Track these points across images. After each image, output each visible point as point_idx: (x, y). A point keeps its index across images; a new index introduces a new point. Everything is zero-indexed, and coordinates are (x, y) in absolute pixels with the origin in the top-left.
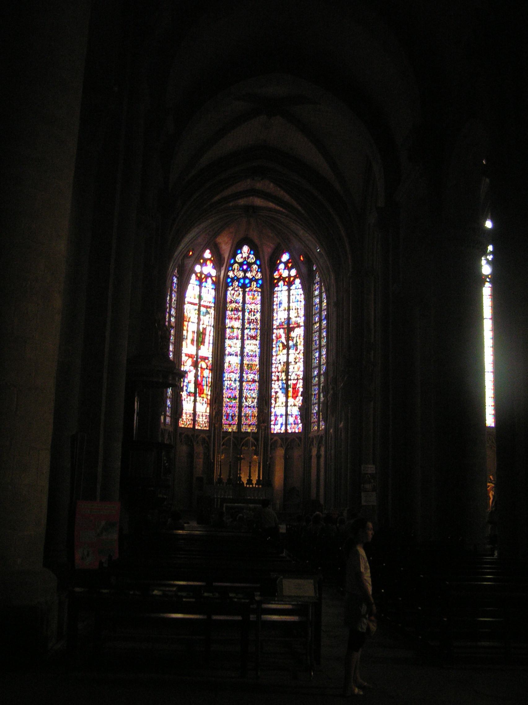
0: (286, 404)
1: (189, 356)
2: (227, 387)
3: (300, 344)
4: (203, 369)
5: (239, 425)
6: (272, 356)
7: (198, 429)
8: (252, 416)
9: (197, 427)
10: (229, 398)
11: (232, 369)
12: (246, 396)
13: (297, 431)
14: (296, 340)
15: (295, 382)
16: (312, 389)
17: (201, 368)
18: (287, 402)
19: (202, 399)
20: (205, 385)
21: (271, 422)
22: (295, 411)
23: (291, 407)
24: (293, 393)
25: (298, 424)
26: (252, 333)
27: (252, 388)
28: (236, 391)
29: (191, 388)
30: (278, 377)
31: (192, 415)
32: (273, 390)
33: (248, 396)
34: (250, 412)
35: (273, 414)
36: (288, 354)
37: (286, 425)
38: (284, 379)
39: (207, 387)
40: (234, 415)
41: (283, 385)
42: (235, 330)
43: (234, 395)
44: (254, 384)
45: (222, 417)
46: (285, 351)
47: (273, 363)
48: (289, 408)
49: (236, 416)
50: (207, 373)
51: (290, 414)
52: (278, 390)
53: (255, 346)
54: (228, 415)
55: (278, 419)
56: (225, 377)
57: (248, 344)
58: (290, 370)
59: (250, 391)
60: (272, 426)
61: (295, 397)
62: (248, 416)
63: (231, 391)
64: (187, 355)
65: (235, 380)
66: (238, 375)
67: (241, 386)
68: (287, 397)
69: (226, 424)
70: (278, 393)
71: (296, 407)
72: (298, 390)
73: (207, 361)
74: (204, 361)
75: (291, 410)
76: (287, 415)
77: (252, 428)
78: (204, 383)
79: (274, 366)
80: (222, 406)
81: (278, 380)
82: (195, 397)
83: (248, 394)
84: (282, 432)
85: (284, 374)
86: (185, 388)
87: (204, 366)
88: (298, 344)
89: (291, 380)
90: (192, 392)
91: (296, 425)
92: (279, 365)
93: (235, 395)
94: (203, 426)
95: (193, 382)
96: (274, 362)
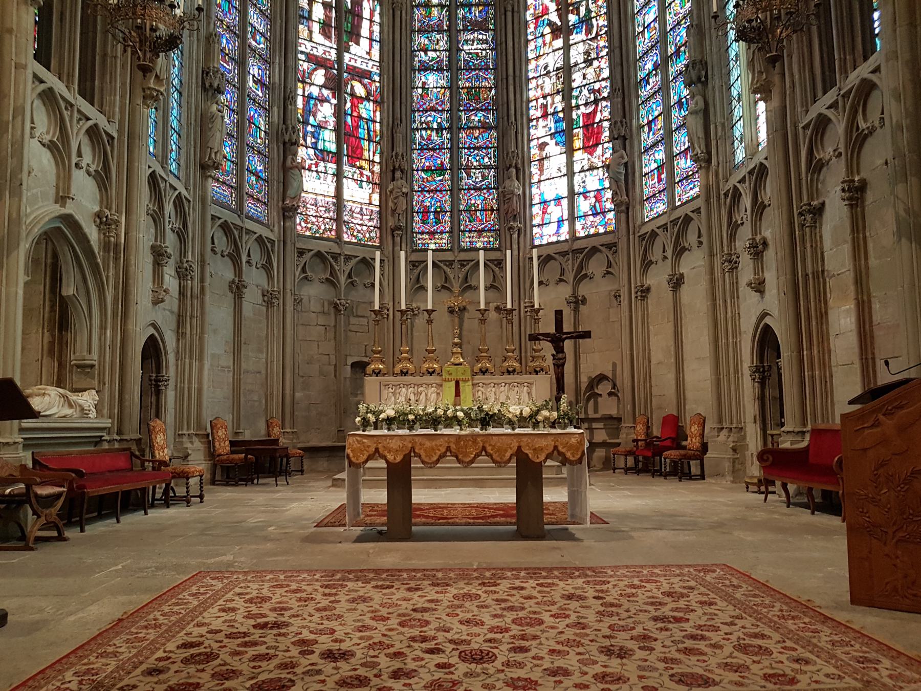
0: (567, 170)
1: (319, 62)
2: (419, 144)
3: (598, 15)
4: (358, 98)
5: (455, 232)
6: (528, 61)
7: (350, 243)
8: (485, 210)
9: (346, 238)
10: (426, 170)
11: (432, 100)
12: (467, 165)
13: (602, 230)
14: (587, 6)
15: (590, 109)
16: (643, 112)
17: (353, 95)
18: (570, 164)
19: (358, 172)
20: (364, 139)
21: (531, 220)
22: (594, 181)
23: (582, 174)
24: (587, 138)
25: (604, 213)
26: (476, 12)
27: (481, 142)
28: (444, 154)
29: (329, 140)
30: (544, 107)
31: (333, 208)
32: (533, 143)
33: (472, 163)
34: (479, 202)
35: (536, 200)
36: (567, 47)
37: (572, 218)
38: (559, 108)
39: (371, 143)
40: (441, 211)
41: (558, 124)
42: (435, 12)
43: (439, 162)
44: (486, 135)
45: (413, 217)
46: (559, 43)
47: (530, 77)
48: (577, 179)
49: (447, 211)
50: (367, 109)
51: (581, 190)
52: (547, 139)
53: (484, 46)
54: (426, 212)
55: (549, 211)
56: (415, 121)
57: (467, 41)
58: (574, 85)
59: (476, 152)
60: (535, 230)
61: (589, 149)
62: (476, 211)
63: (431, 153)
64: (310, 58)
65: (440, 129)
66: (445, 115)
67: (454, 140)
68: (570, 151)
69: (422, 233)
70: (547, 148)
71: (595, 171)
72: (600, 127)
73: (366, 81)
74: (360, 82)
75: (584, 182)
76: (572, 194)
77: (486, 239)
78: (362, 133)
79: (532, 85)
80: (412, 190)
81: (545, 116)
82: (339, 163)
83: (470, 158)
84: (562, 238)
85: (558, 98)
86: (309, 140)
87: (360, 90)
88: (593, 14)
89: (578, 107)
90: (331, 152)
91: (598, 217)
92: (546, 79)
93: (442, 163)
94: (364, 237)
95: (331, 126)
96: (531, 75)
